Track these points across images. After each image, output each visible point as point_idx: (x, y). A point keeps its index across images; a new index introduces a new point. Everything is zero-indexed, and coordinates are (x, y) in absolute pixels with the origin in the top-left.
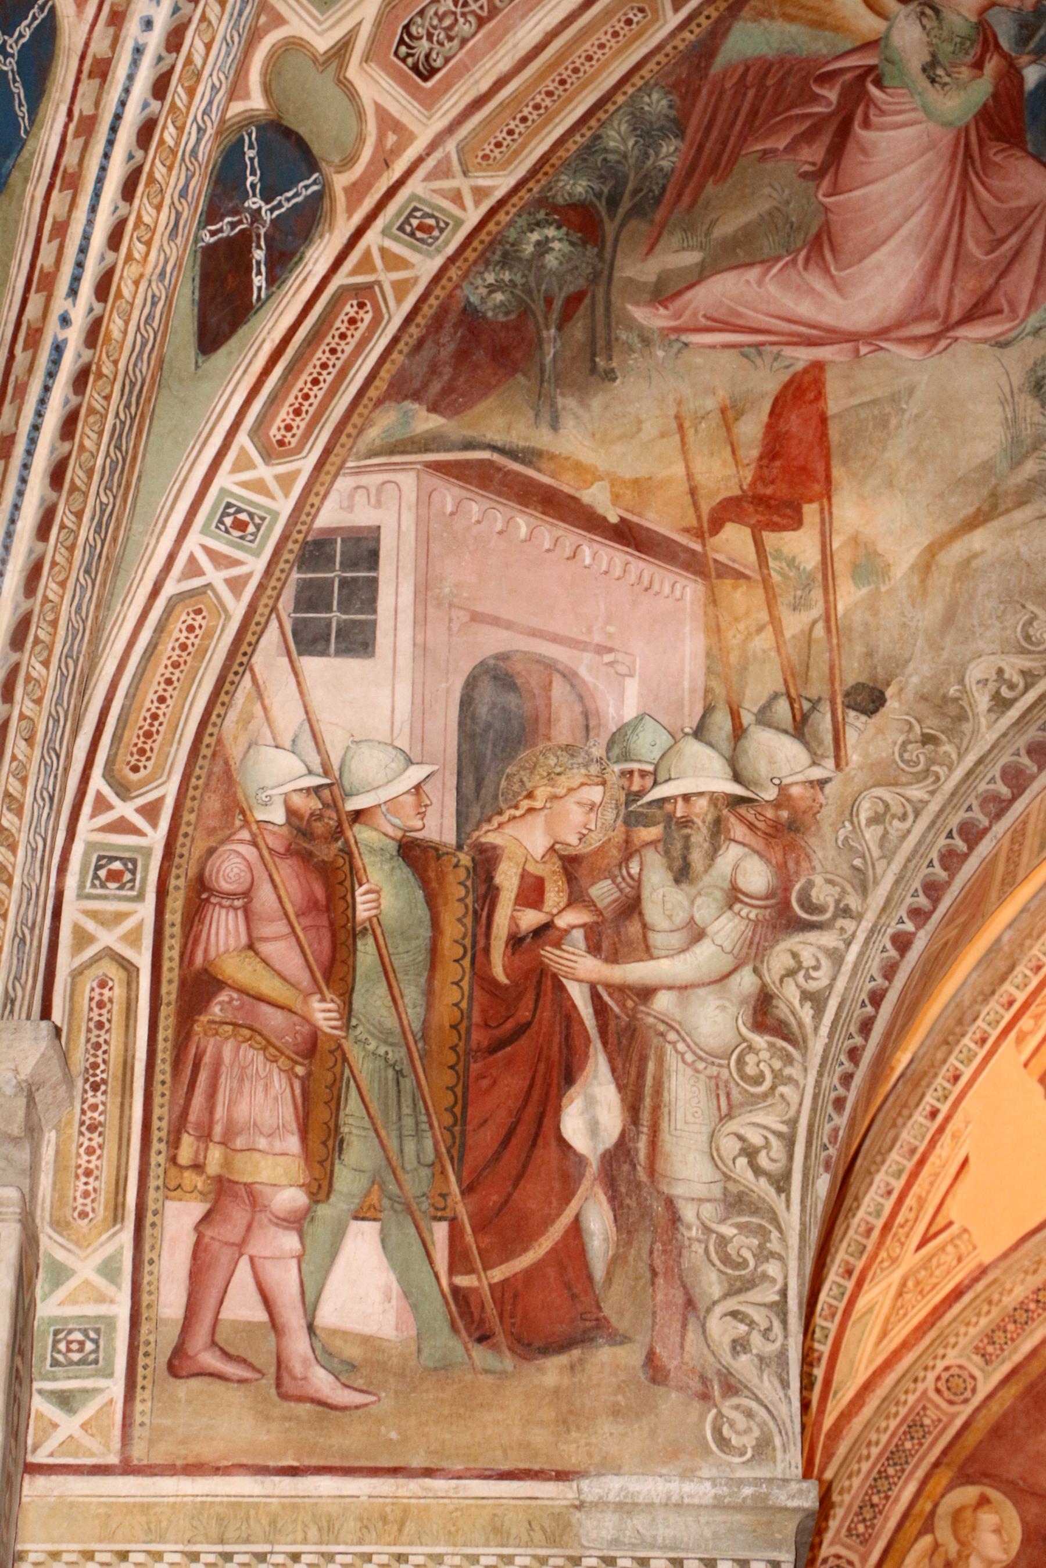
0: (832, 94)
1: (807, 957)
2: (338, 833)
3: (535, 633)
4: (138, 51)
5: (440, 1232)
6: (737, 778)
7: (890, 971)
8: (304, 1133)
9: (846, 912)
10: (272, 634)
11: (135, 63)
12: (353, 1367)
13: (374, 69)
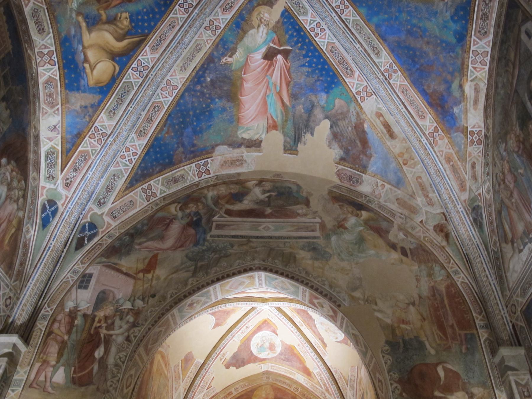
0: (168, 221)
2: (75, 313)
3: (110, 287)
4: (68, 211)
5: (73, 369)
6: (133, 306)
7: (147, 333)
8: (58, 353)
10: (75, 287)
11: (67, 213)
12: (54, 387)
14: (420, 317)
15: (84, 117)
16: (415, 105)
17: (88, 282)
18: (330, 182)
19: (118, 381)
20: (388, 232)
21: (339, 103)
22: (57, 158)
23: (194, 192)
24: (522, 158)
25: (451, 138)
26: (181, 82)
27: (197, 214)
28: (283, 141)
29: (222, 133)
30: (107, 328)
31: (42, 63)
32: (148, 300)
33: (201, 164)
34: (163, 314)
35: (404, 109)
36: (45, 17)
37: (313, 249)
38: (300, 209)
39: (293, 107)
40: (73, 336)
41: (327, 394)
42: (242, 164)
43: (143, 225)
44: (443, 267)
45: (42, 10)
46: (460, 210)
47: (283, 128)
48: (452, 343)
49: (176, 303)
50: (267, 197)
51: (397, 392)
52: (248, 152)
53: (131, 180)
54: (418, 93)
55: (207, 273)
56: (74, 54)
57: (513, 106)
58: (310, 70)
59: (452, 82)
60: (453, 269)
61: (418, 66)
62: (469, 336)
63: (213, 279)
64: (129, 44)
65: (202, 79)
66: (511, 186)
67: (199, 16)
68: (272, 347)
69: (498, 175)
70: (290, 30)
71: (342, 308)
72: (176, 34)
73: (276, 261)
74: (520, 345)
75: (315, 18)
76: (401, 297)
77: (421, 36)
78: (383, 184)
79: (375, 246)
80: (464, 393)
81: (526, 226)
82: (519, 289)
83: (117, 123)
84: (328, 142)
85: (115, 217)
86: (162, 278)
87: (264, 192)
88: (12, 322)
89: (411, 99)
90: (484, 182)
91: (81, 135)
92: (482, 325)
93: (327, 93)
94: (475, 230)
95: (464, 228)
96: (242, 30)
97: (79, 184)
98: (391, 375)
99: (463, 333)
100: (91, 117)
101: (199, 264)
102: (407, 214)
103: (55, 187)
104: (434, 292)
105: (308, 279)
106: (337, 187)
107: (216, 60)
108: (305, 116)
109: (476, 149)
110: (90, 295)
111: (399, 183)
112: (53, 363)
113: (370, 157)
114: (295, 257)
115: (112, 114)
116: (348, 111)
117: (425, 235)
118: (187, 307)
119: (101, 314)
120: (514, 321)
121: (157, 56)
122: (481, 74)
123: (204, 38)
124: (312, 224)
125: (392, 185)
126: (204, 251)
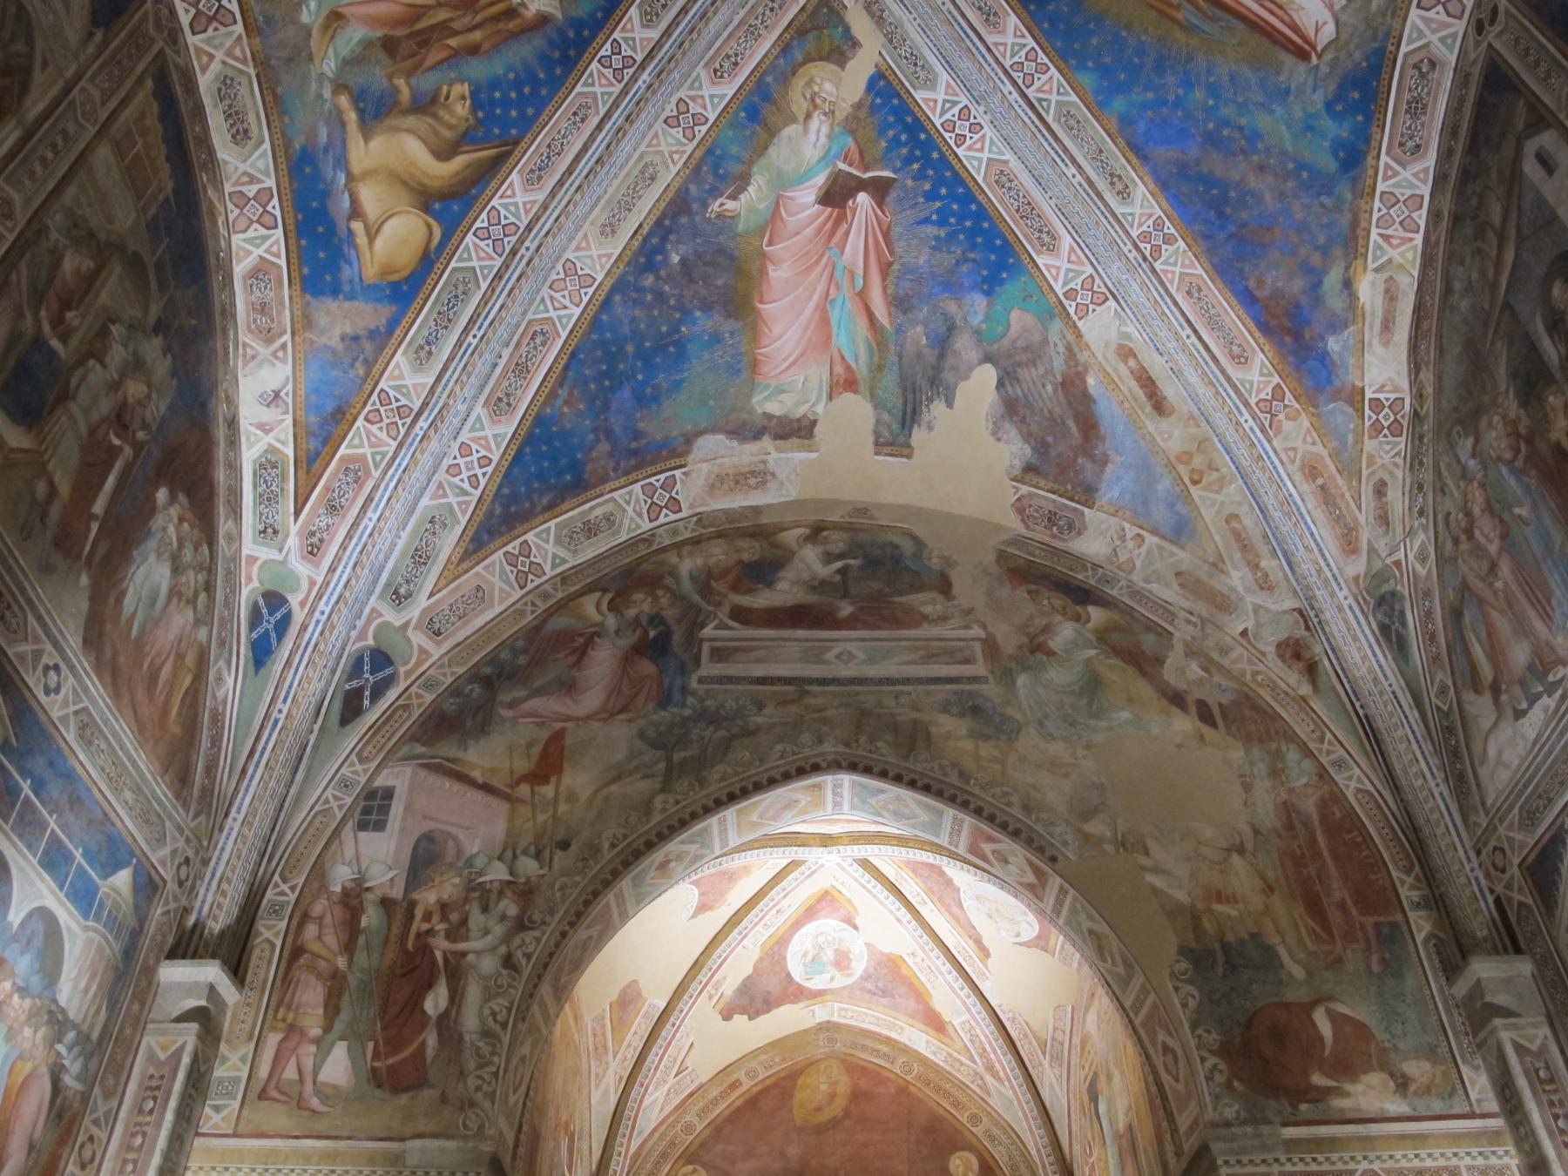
0: (582, 640)
1: (528, 940)
2: (359, 895)
3: (447, 823)
5: (371, 1045)
6: (511, 874)
7: (557, 945)
8: (326, 1007)
9: (544, 923)
10: (350, 824)
12: (327, 1097)
13: (418, 632)
14: (1259, 883)
15: (352, 366)
16: (1221, 328)
17: (385, 810)
18: (998, 528)
19: (496, 1074)
20: (1159, 661)
21: (1019, 320)
22: (284, 477)
23: (640, 561)
24: (1526, 479)
25: (1319, 416)
26: (602, 267)
27: (657, 619)
28: (872, 421)
29: (711, 403)
30: (451, 935)
31: (242, 224)
32: (551, 860)
33: (658, 485)
34: (596, 894)
35: (1194, 338)
36: (252, 99)
37: (974, 709)
38: (928, 602)
39: (899, 330)
40: (361, 958)
41: (989, 1078)
42: (764, 483)
43: (515, 652)
44: (1308, 753)
45: (244, 81)
46: (1345, 604)
47: (872, 388)
49: (627, 864)
50: (839, 571)
52: (779, 451)
53: (476, 533)
54: (1233, 299)
55: (702, 782)
56: (325, 195)
57: (1499, 344)
58: (942, 234)
59: (1325, 272)
60: (1333, 757)
61: (1232, 228)
62: (1386, 930)
63: (717, 795)
64: (469, 166)
65: (659, 258)
66: (1493, 548)
67: (654, 92)
68: (842, 961)
69: (1452, 517)
70: (891, 126)
71: (1057, 866)
72: (592, 138)
73: (879, 744)
74: (1518, 950)
75: (956, 95)
76: (1209, 832)
77: (1243, 152)
78: (1139, 535)
79: (1130, 700)
80: (1385, 1076)
81: (1537, 652)
82: (1516, 810)
83: (438, 379)
84: (991, 425)
85: (438, 633)
86: (584, 795)
87: (829, 558)
88: (195, 925)
89: (1212, 312)
90: (1410, 533)
91: (344, 414)
93: (988, 293)
95: (1359, 649)
96: (765, 125)
97: (343, 547)
98: (1199, 1037)
99: (1369, 921)
100: (369, 365)
101: (678, 757)
102: (1204, 614)
103: (280, 558)
105: (966, 792)
106: (1018, 541)
107: (695, 206)
108: (930, 355)
109: (1388, 448)
110: (393, 845)
111: (1180, 531)
112: (316, 1032)
113: (1104, 462)
114: (928, 733)
115: (423, 354)
116: (1045, 341)
118: (652, 874)
119: (428, 898)
120: (1499, 889)
121: (541, 197)
122: (1402, 254)
123: (664, 148)
125: (1164, 538)
126: (685, 720)
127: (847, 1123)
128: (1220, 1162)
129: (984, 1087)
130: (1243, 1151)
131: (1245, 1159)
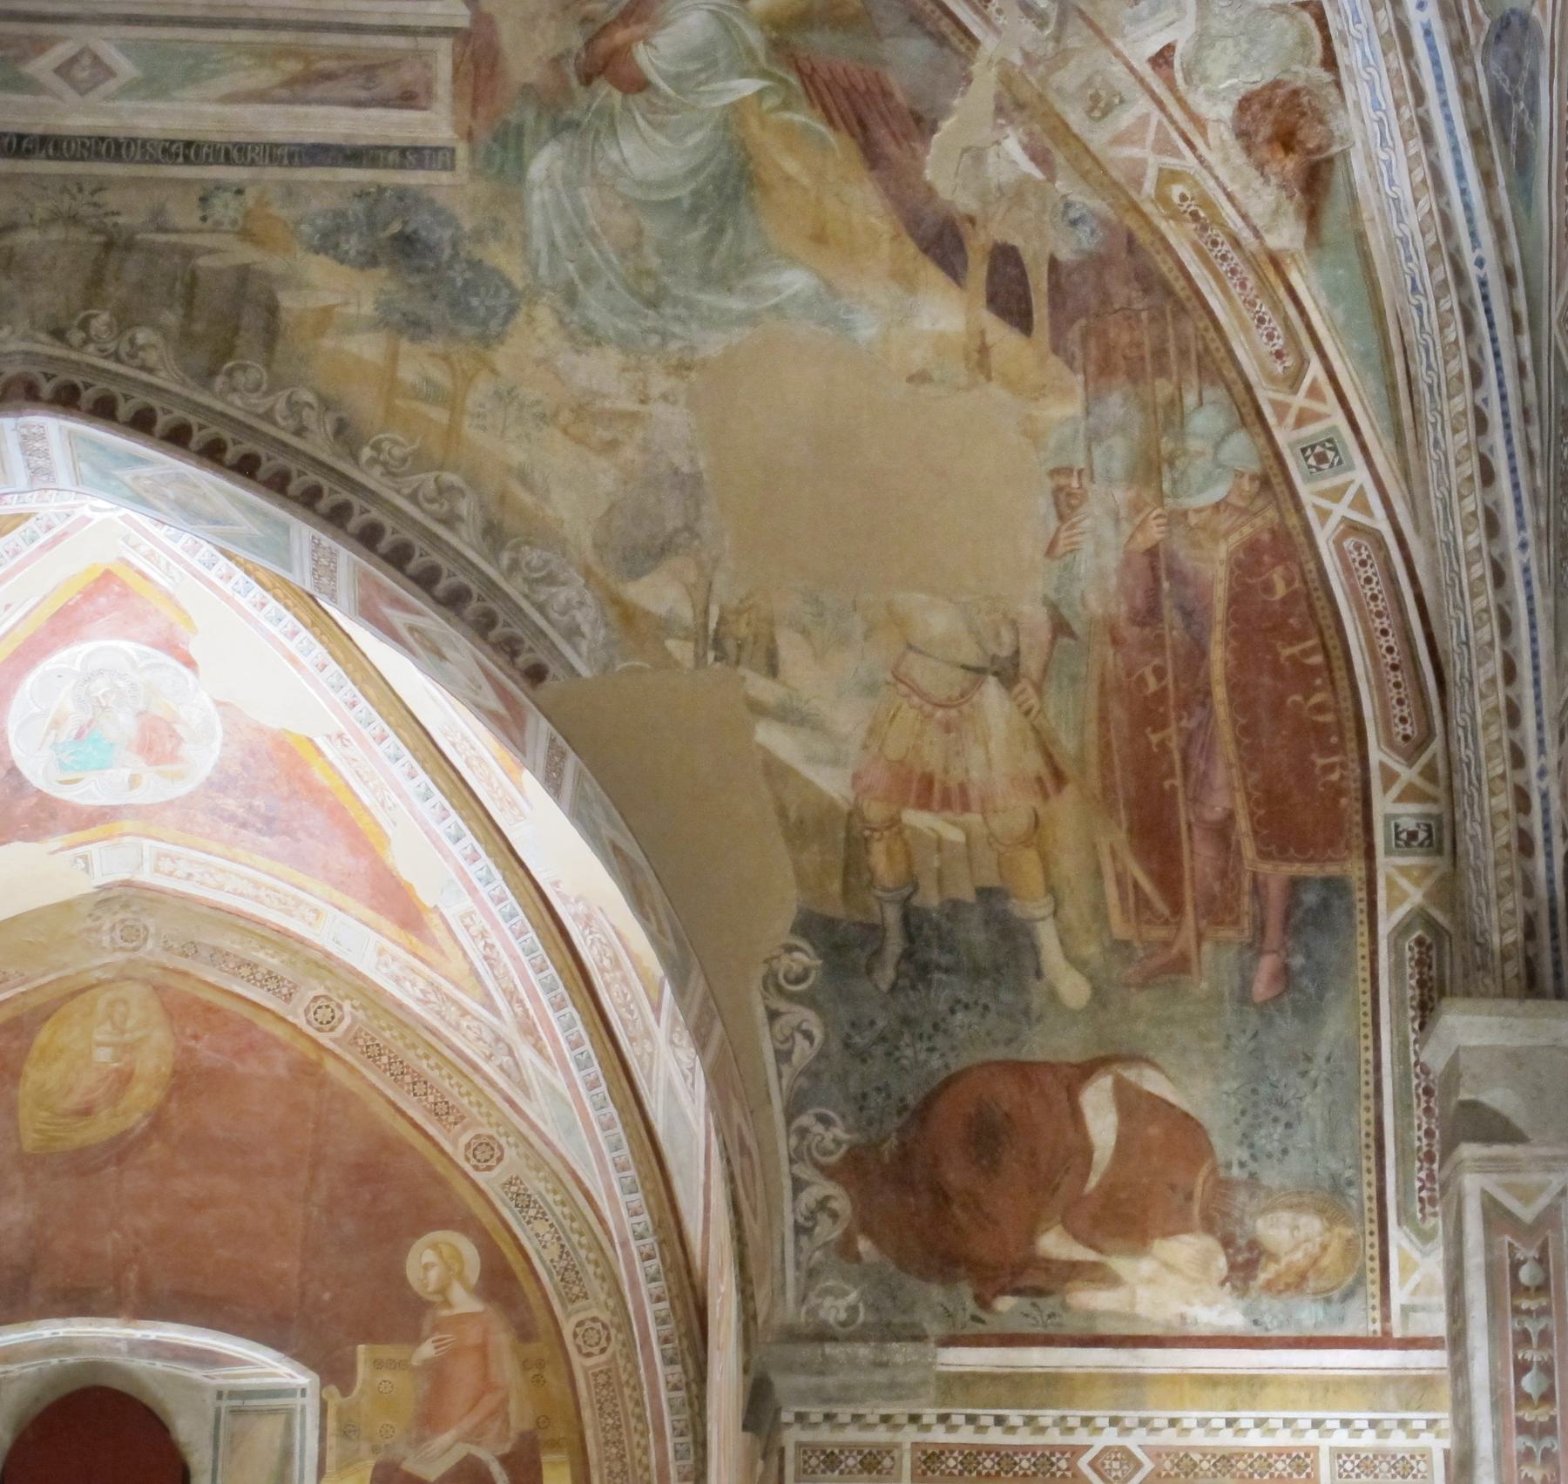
14: (1034, 763)
20: (922, 124)
41: (526, 1053)
44: (1250, 415)
48: (1200, 937)
51: (828, 1231)
60: (1311, 430)
62: (1310, 898)
73: (142, 336)
79: (820, 238)
80: (1210, 1243)
92: (1409, 824)
94: (1487, 178)
99: (1278, 873)
104: (1153, 592)
105: (344, 479)
114: (272, 309)
117: (1170, 162)
124: (402, 42)
127: (156, 1149)
128: (787, 1417)
129: (514, 1071)
130: (846, 1395)
131: (844, 1413)
